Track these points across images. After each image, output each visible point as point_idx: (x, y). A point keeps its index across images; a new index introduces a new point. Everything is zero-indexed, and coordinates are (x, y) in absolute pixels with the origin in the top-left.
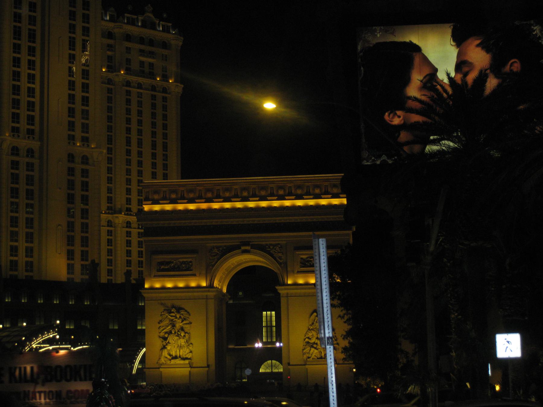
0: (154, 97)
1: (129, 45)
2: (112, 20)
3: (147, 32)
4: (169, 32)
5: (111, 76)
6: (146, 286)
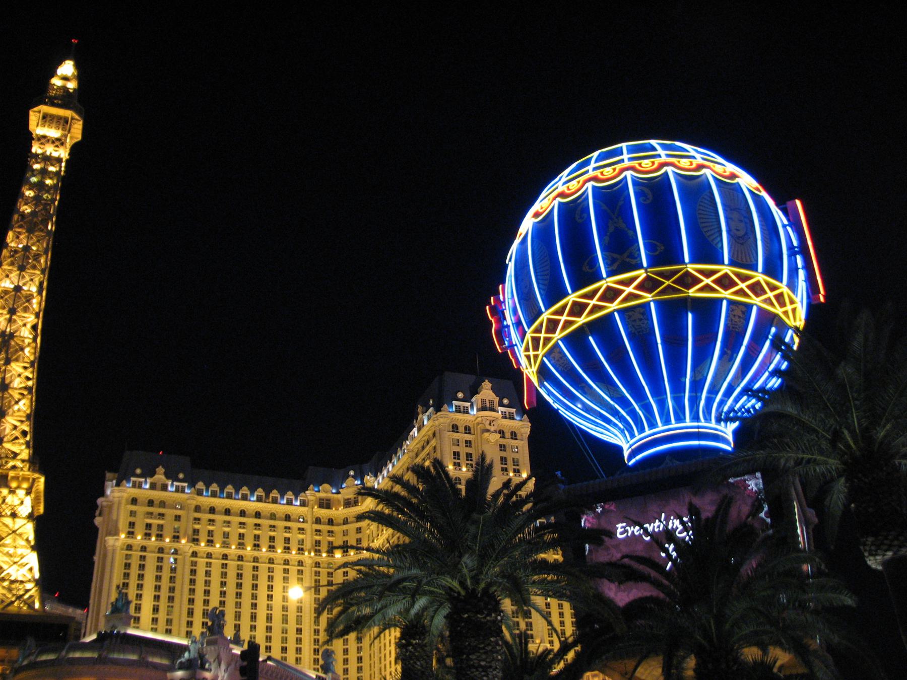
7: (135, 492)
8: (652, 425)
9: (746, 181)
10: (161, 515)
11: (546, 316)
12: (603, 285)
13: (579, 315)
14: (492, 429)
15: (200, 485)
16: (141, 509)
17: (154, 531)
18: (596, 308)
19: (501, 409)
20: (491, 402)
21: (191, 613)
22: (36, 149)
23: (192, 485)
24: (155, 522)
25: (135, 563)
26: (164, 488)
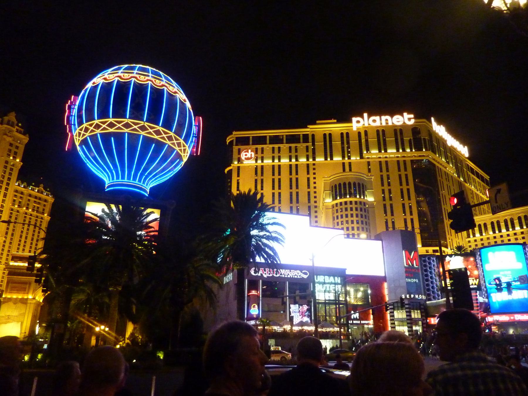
0: (36, 220)
1: (30, 198)
2: (24, 187)
3: (39, 195)
4: (48, 196)
5: (19, 209)
6: (4, 296)
8: (123, 178)
9: (188, 104)
11: (97, 121)
12: (126, 121)
13: (111, 127)
14: (9, 134)
18: (119, 128)
19: (16, 127)
20: (13, 123)
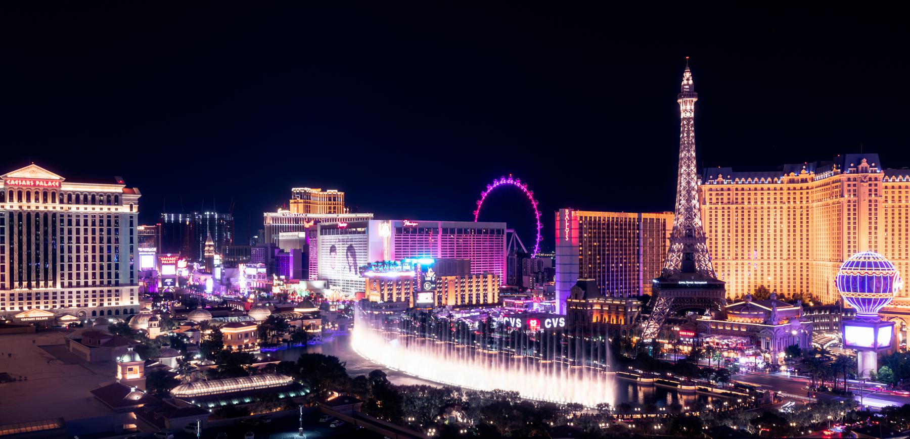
7: (711, 186)
10: (722, 194)
15: (737, 179)
16: (714, 193)
17: (720, 201)
21: (737, 231)
22: (683, 115)
23: (734, 181)
24: (720, 197)
25: (713, 214)
26: (722, 183)
